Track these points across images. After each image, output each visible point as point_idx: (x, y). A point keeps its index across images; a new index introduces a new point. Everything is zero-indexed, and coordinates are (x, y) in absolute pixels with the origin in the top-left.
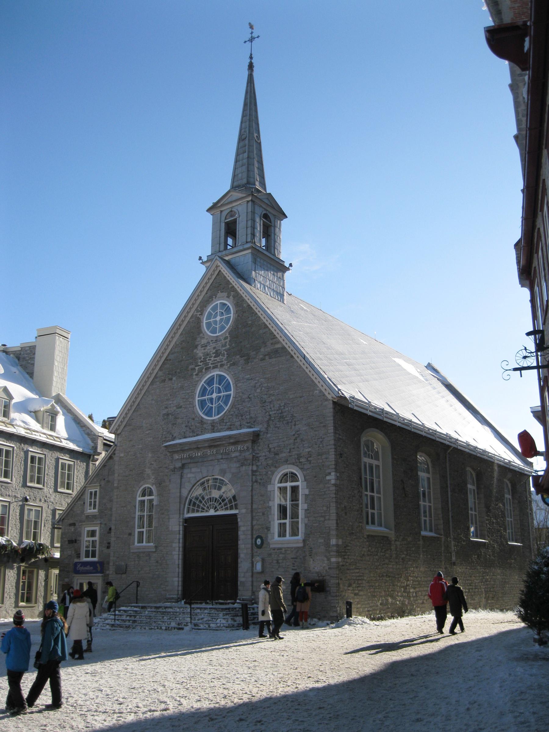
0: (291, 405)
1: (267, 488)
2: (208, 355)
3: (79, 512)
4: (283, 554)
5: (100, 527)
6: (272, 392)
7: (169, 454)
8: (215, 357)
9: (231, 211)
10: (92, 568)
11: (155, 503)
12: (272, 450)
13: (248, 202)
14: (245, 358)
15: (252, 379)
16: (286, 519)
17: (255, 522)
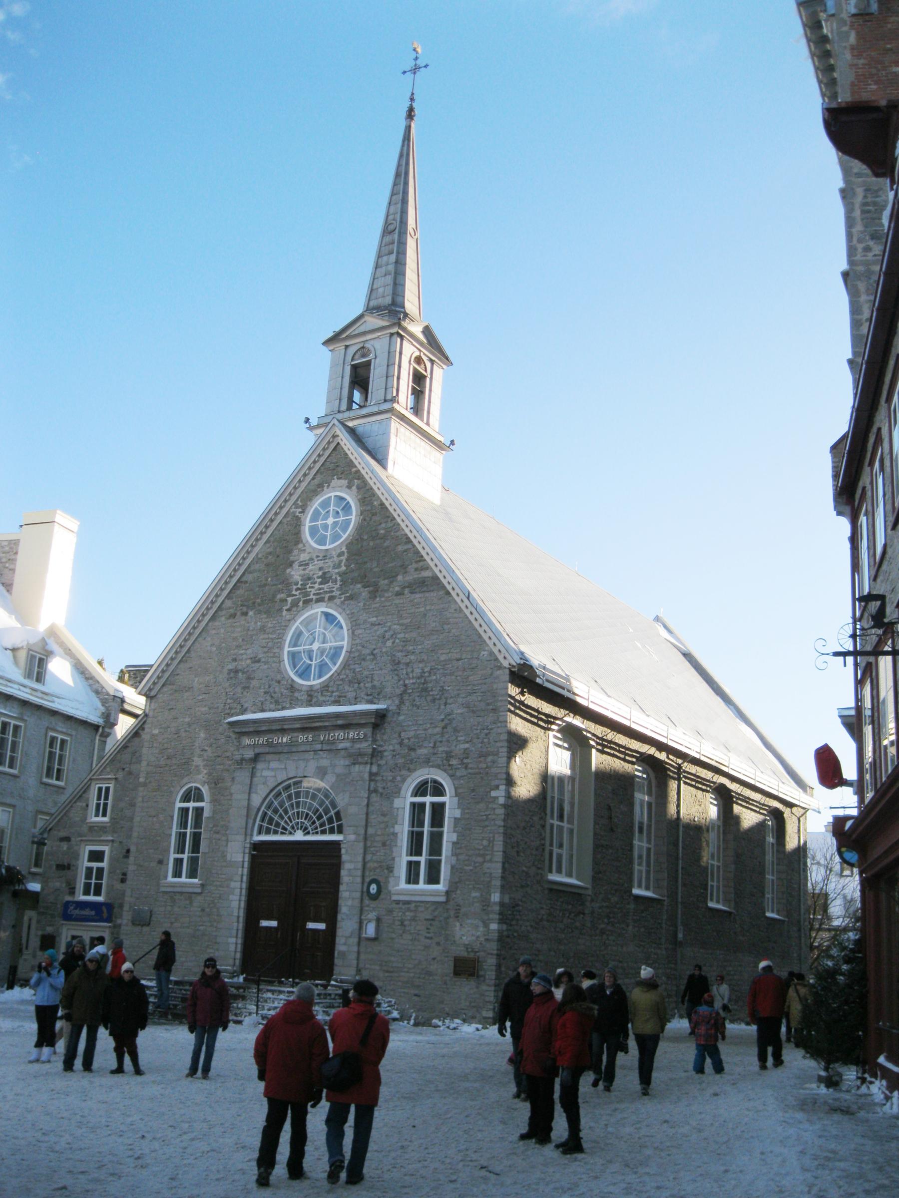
0: (441, 671)
1: (392, 803)
2: (309, 579)
3: (77, 819)
4: (411, 911)
5: (112, 846)
6: (411, 648)
7: (233, 736)
8: (321, 583)
9: (363, 347)
10: (93, 913)
11: (206, 814)
12: (406, 741)
13: (392, 334)
14: (371, 589)
15: (379, 624)
16: (421, 855)
17: (369, 857)
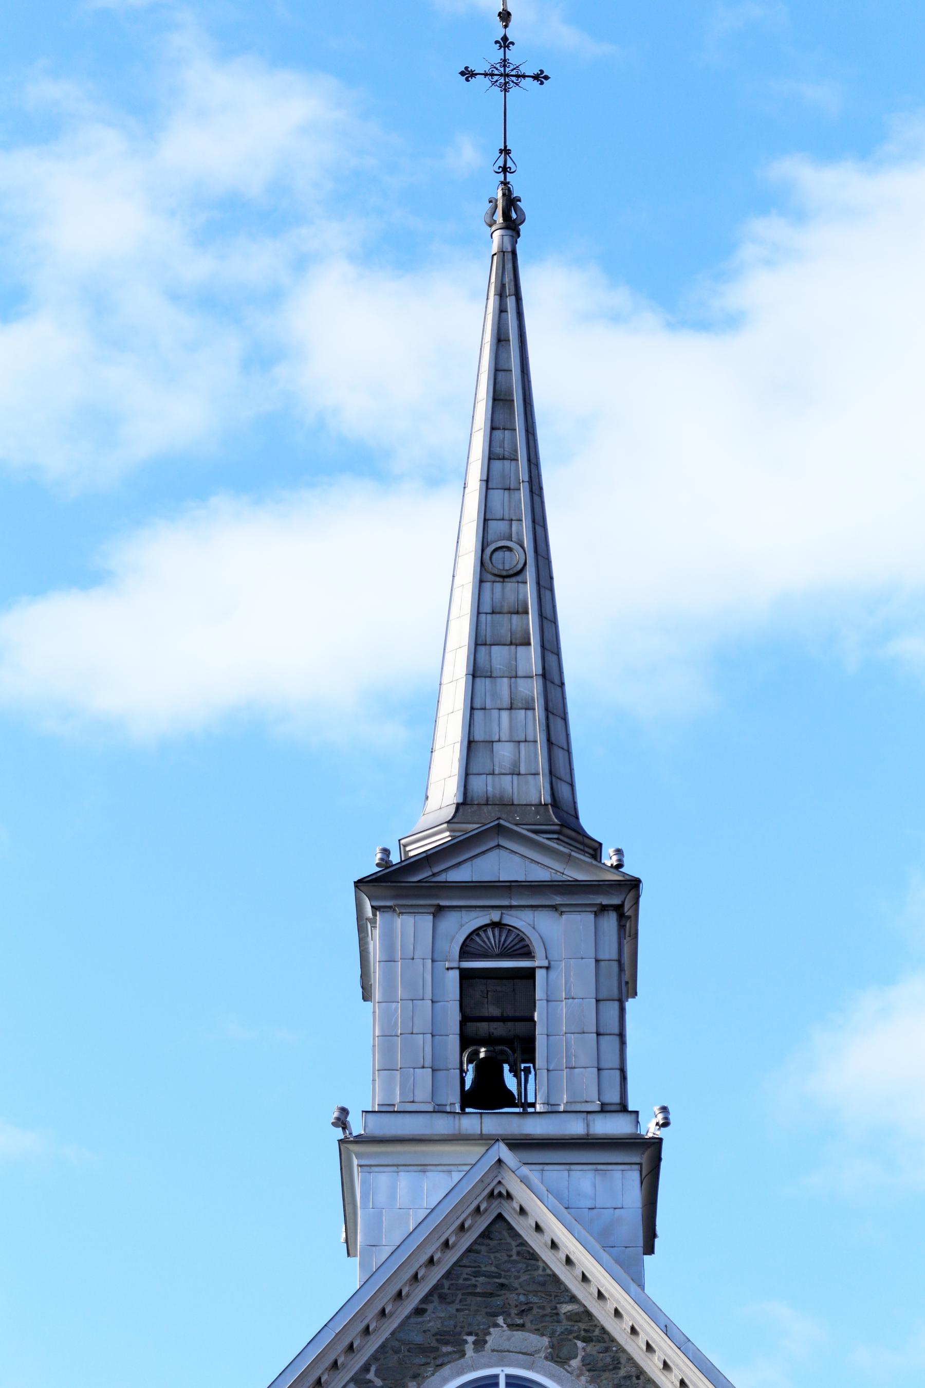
9: (497, 925)
